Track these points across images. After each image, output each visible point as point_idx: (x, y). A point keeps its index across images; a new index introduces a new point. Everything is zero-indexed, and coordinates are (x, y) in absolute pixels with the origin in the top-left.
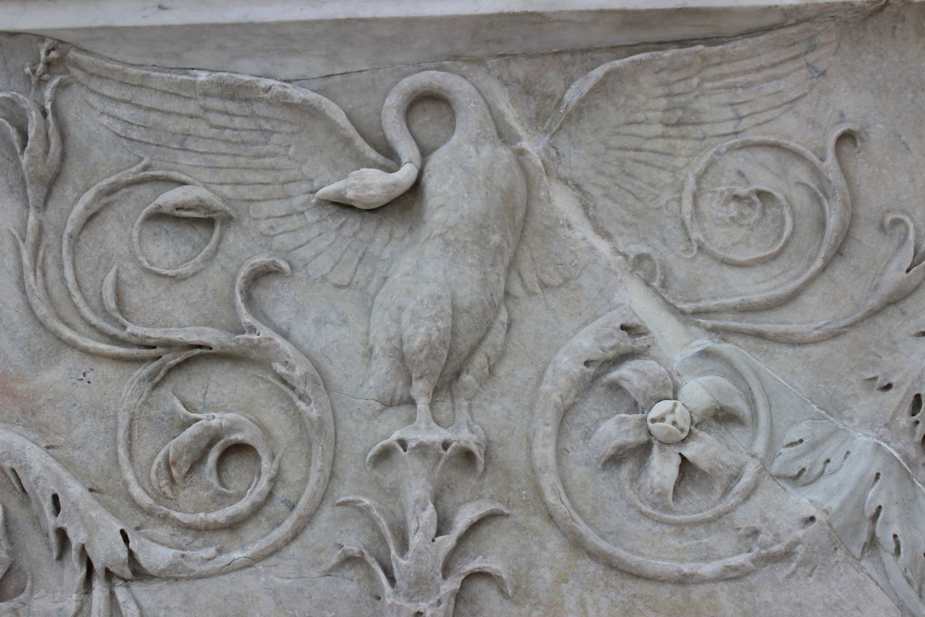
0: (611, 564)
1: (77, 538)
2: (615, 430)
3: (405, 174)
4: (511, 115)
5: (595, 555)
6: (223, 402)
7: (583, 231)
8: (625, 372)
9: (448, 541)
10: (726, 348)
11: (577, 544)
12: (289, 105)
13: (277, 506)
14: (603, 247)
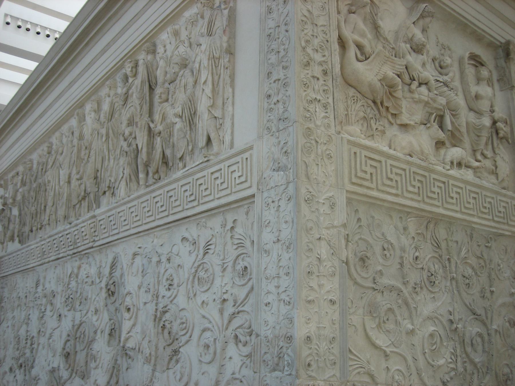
2: (499, 268)
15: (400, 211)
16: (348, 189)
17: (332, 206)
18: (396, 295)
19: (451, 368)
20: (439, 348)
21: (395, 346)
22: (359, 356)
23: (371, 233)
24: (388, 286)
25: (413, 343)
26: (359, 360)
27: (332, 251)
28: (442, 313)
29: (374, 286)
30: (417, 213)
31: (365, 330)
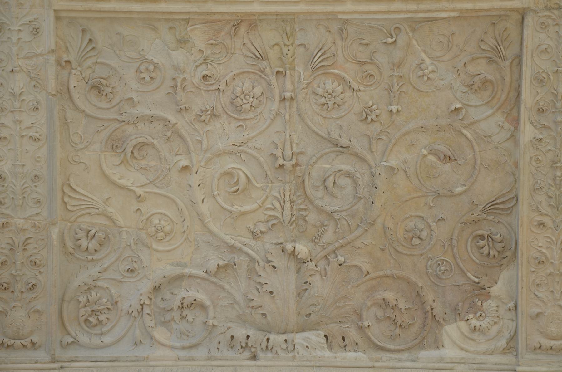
0: (418, 90)
1: (352, 86)
2: (420, 73)
3: (394, 39)
4: (408, 30)
5: (417, 89)
6: (370, 69)
7: (417, 46)
8: (421, 66)
9: (398, 87)
10: (434, 62)
11: (414, 87)
12: (378, 28)
13: (377, 83)
14: (419, 48)
15: (166, 20)
16: (56, 9)
17: (36, 32)
18: (161, 126)
19: (270, 216)
20: (244, 190)
21: (157, 187)
22: (90, 196)
23: (116, 54)
24: (143, 116)
25: (190, 184)
26: (90, 200)
27: (34, 83)
28: (258, 146)
29: (119, 118)
30: (203, 17)
31: (100, 167)
